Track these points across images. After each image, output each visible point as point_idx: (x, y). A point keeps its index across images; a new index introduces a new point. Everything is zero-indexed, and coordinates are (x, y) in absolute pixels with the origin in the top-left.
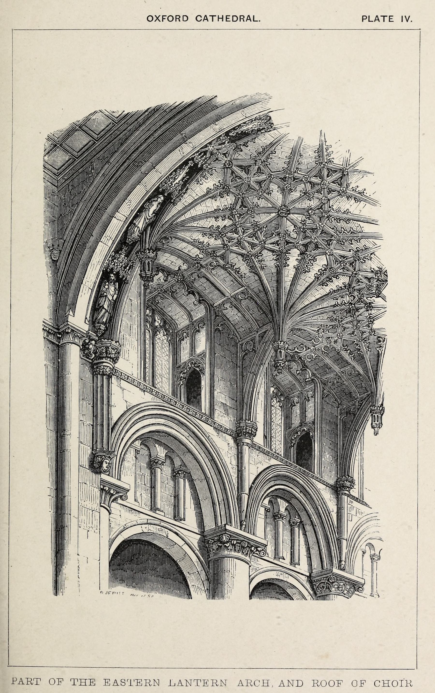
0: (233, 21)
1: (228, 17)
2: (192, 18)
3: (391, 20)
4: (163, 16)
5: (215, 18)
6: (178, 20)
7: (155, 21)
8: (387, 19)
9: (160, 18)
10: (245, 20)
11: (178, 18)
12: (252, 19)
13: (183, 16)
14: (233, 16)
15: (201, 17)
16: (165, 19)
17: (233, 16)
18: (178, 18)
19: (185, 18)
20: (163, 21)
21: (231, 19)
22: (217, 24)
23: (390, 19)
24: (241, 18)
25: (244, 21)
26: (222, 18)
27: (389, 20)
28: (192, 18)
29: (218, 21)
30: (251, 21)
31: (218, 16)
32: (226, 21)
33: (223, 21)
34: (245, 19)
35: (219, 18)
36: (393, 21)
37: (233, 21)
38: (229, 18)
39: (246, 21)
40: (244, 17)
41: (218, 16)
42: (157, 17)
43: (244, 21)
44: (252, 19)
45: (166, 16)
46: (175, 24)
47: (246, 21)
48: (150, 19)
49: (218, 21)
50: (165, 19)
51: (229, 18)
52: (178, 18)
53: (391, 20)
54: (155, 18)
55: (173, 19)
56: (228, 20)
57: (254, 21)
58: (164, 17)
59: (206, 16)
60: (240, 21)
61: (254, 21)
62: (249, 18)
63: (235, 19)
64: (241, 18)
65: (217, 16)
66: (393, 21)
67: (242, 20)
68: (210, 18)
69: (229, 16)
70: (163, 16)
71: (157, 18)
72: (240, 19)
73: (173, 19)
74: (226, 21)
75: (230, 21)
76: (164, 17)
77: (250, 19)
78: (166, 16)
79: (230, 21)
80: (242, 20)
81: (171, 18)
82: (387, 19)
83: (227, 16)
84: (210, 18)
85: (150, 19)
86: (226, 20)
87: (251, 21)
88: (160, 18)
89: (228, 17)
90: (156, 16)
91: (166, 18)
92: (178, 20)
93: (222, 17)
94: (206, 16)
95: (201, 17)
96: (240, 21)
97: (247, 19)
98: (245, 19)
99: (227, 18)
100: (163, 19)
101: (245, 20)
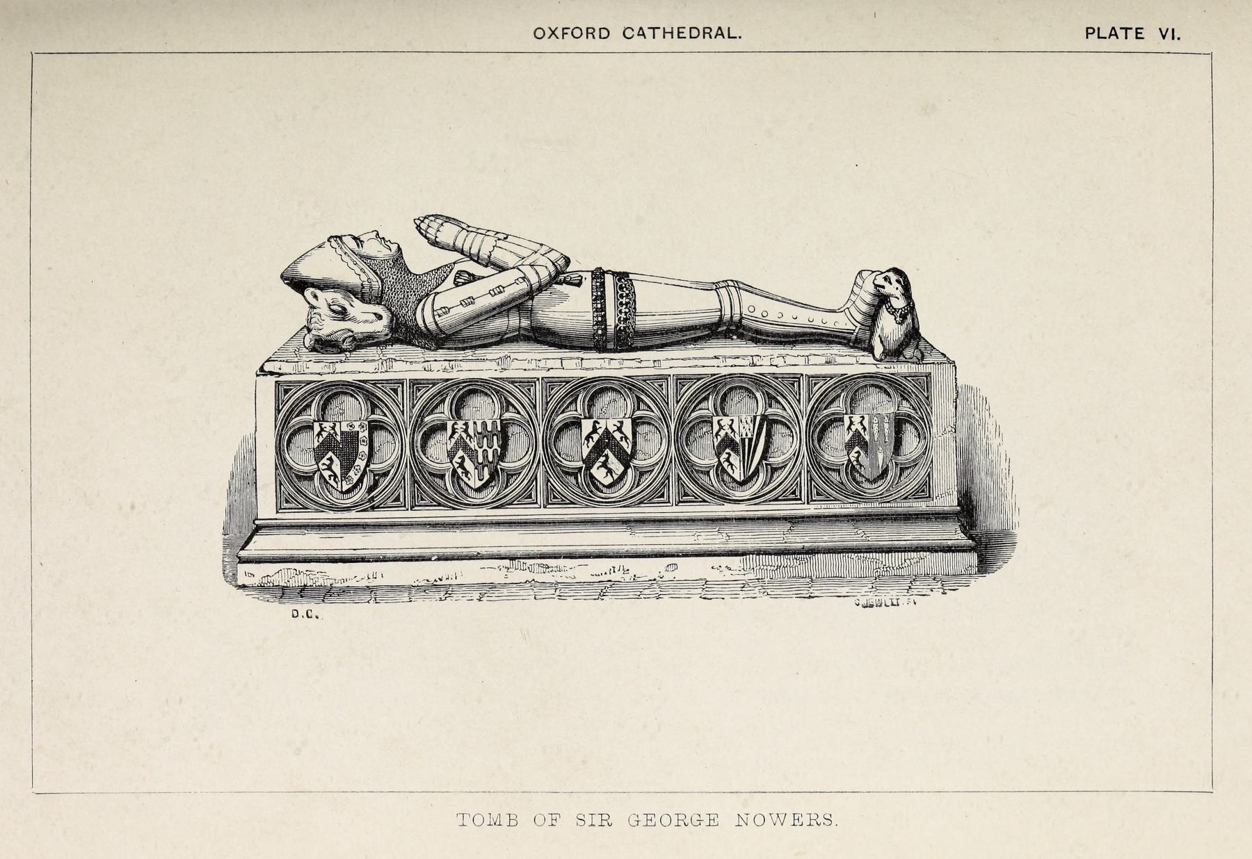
0: (691, 37)
1: (681, 30)
2: (616, 33)
3: (1139, 36)
4: (563, 29)
5: (659, 33)
6: (590, 36)
7: (549, 38)
8: (1132, 33)
9: (559, 32)
10: (713, 36)
11: (590, 32)
12: (726, 35)
13: (600, 29)
14: (691, 28)
15: (633, 30)
16: (567, 34)
17: (691, 28)
18: (590, 32)
19: (604, 33)
20: (563, 38)
21: (687, 34)
22: (660, 43)
23: (1137, 33)
24: (706, 32)
25: (711, 37)
26: (672, 33)
27: (1137, 36)
28: (616, 33)
29: (664, 37)
30: (724, 37)
31: (664, 29)
32: (679, 37)
33: (672, 38)
34: (713, 34)
35: (664, 32)
36: (1143, 38)
37: (691, 37)
38: (683, 33)
39: (715, 37)
40: (711, 30)
41: (664, 29)
42: (553, 30)
43: (711, 37)
44: (726, 35)
45: (569, 28)
46: (585, 43)
47: (715, 37)
48: (538, 34)
49: (664, 37)
50: (567, 34)
51: (683, 33)
52: (592, 33)
53: (1139, 36)
54: (548, 33)
55: (582, 34)
56: (681, 35)
57: (729, 37)
58: (565, 31)
59: (641, 28)
60: (704, 37)
61: (729, 37)
62: (720, 32)
63: (695, 33)
64: (706, 32)
65: (662, 29)
66: (1143, 38)
67: (707, 36)
68: (649, 33)
69: (684, 28)
70: (563, 29)
71: (553, 33)
72: (704, 33)
73: (582, 34)
74: (679, 37)
75: (685, 38)
76: (565, 31)
77: (722, 34)
78: (569, 28)
79: (685, 38)
80: (707, 36)
81: (577, 33)
82: (1132, 33)
83: (679, 28)
84: (649, 33)
85: (539, 33)
86: (678, 35)
87: (724, 37)
88: (559, 32)
89: (681, 30)
90: (551, 29)
91: (569, 31)
92: (590, 36)
93: (670, 31)
94: (641, 28)
95: (633, 30)
96: (704, 37)
97: (717, 35)
98: (713, 34)
99: (679, 33)
100: (564, 34)
101: (713, 36)
